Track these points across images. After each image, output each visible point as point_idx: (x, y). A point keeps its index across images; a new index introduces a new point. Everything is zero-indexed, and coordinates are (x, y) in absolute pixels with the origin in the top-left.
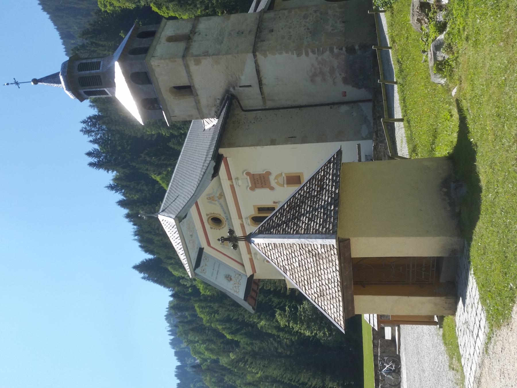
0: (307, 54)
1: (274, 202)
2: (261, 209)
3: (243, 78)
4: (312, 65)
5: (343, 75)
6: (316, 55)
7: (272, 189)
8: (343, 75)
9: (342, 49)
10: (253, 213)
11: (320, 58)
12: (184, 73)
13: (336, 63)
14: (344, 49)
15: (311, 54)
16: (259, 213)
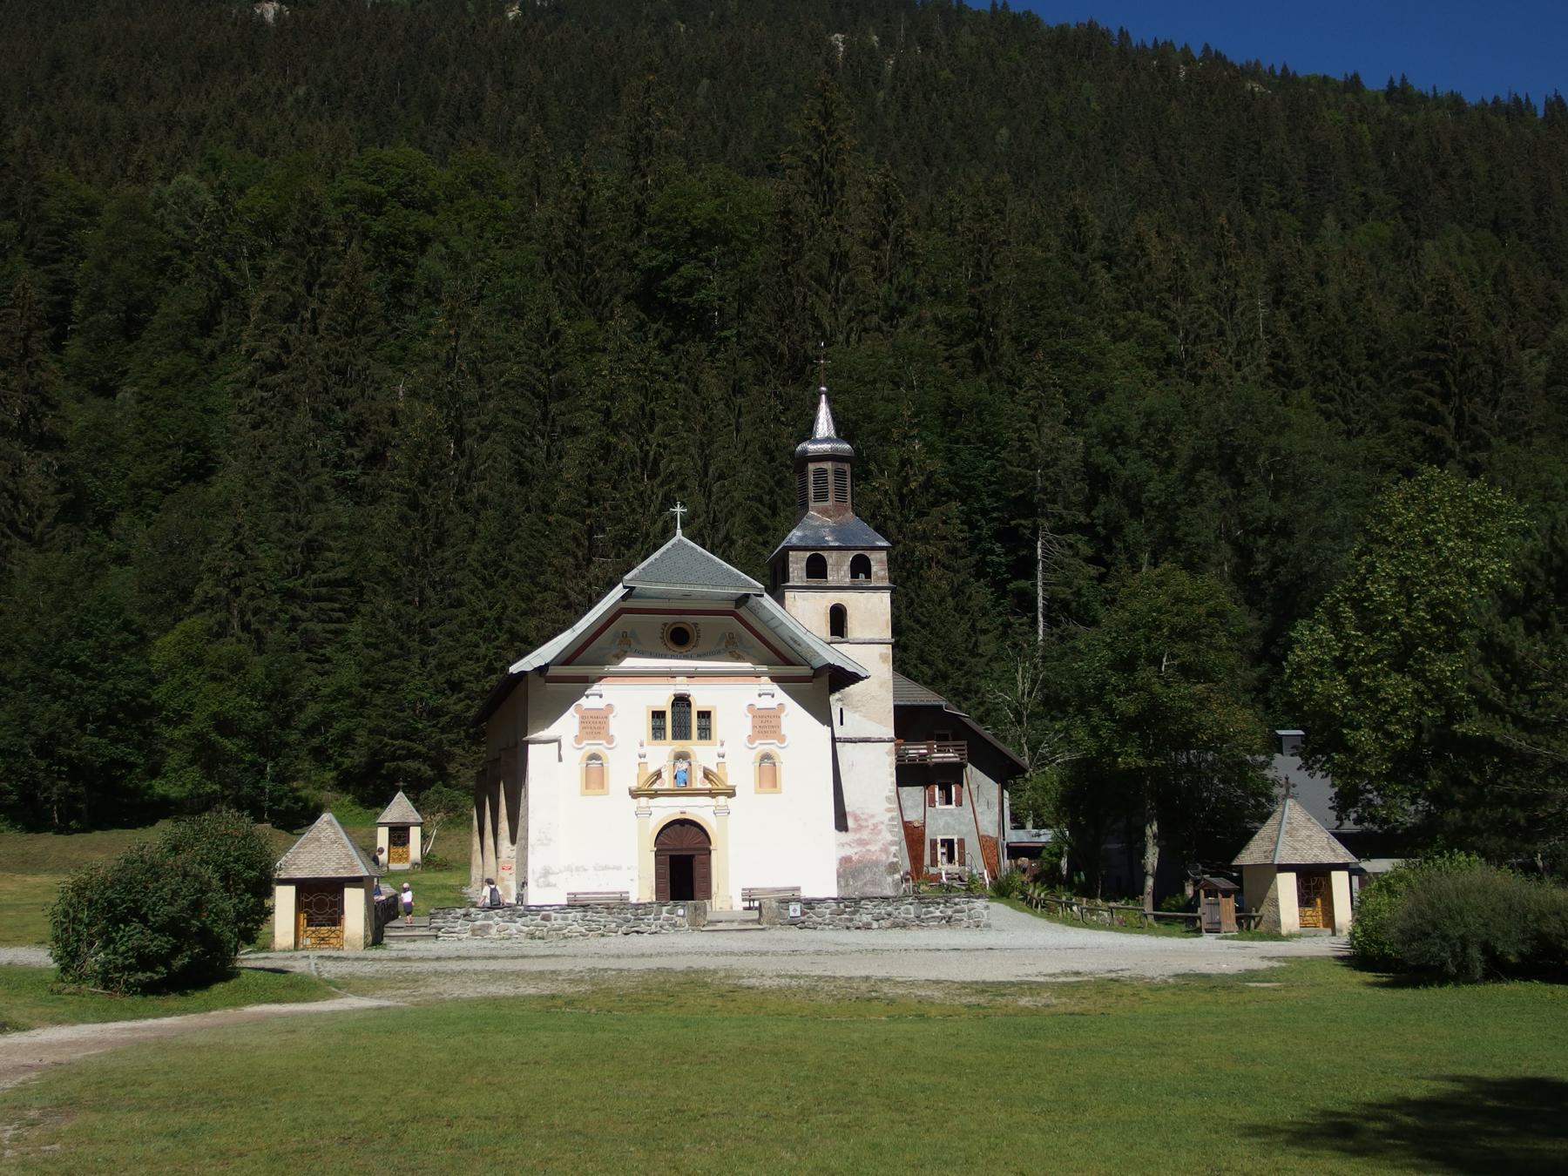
0: (889, 810)
1: (722, 745)
2: (705, 715)
3: (857, 716)
4: (872, 816)
5: (855, 858)
6: (887, 822)
7: (751, 739)
8: (855, 858)
9: (895, 856)
10: (698, 704)
11: (883, 827)
12: (868, 636)
13: (873, 848)
14: (895, 860)
15: (889, 815)
16: (699, 713)
